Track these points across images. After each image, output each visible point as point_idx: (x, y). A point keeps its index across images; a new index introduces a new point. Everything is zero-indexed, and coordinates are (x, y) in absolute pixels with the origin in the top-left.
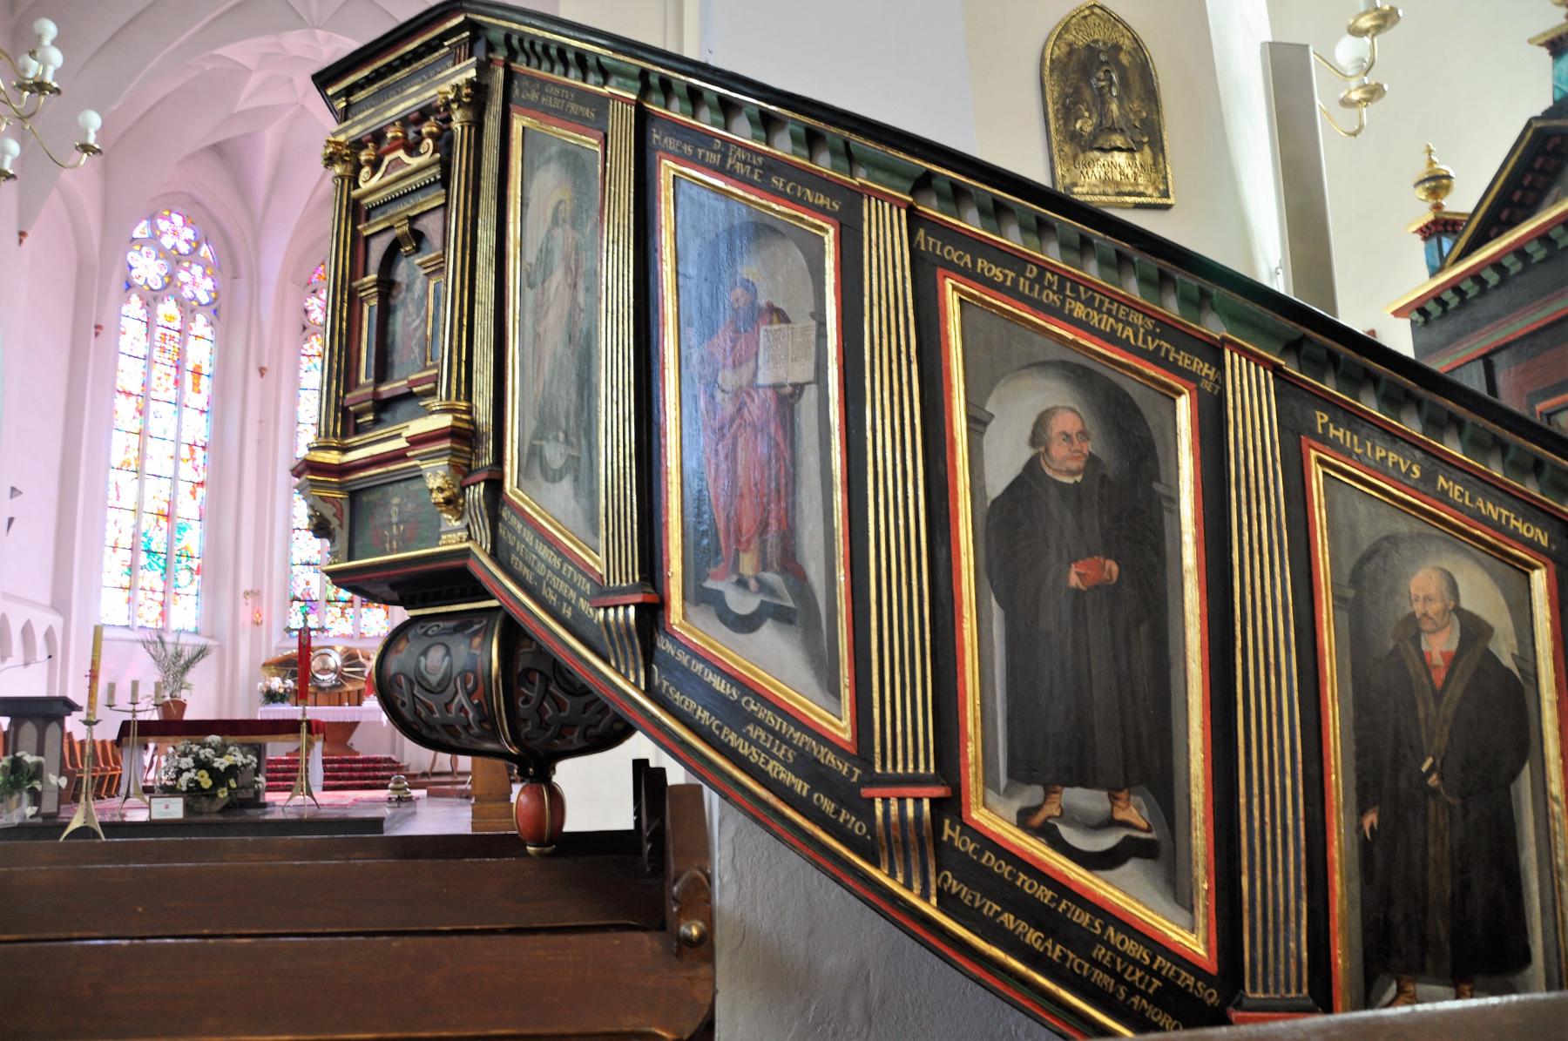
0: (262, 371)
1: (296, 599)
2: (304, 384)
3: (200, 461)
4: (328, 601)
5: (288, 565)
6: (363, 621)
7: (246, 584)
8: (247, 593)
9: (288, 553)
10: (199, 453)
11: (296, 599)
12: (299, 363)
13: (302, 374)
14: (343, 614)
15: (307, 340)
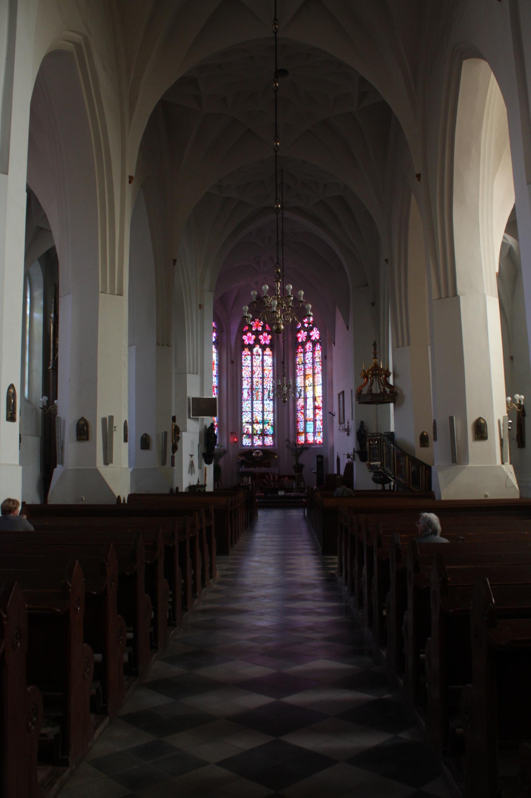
0: (232, 362)
1: (244, 434)
2: (244, 364)
3: (215, 391)
4: (255, 435)
5: (242, 423)
6: (265, 441)
7: (230, 430)
8: (231, 433)
9: (242, 420)
10: (215, 389)
11: (244, 434)
12: (242, 357)
13: (243, 361)
14: (259, 439)
15: (244, 350)
